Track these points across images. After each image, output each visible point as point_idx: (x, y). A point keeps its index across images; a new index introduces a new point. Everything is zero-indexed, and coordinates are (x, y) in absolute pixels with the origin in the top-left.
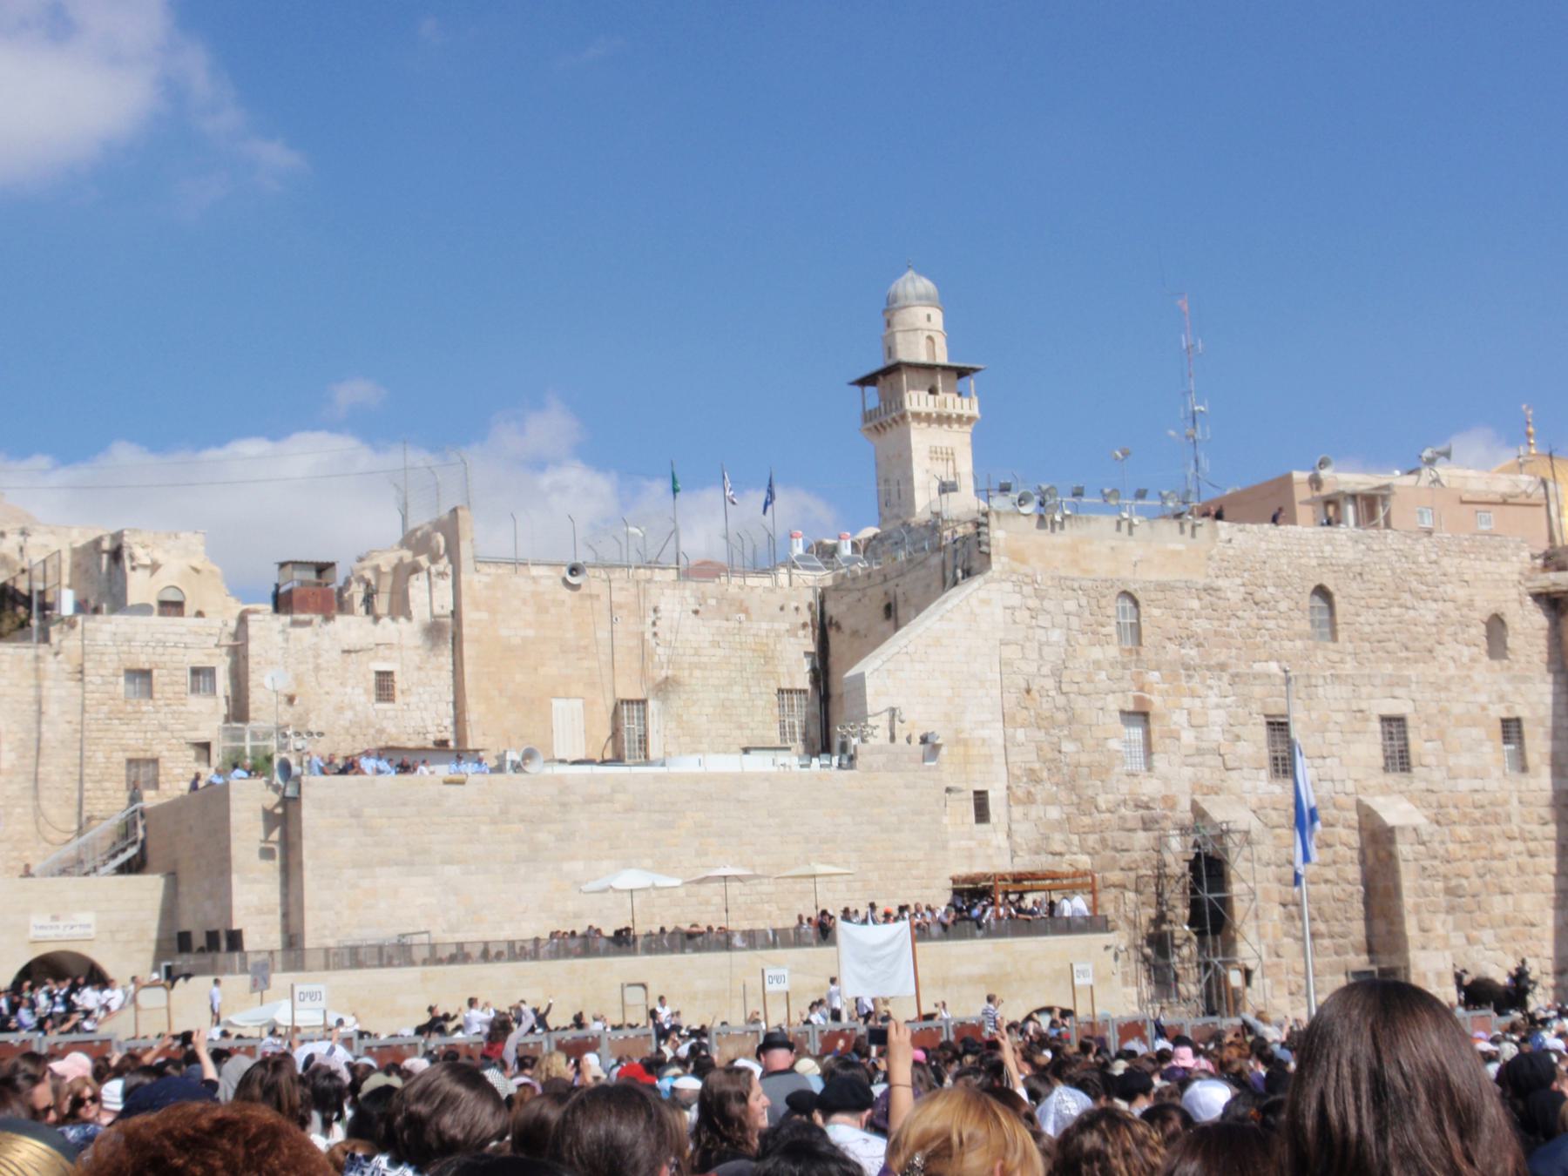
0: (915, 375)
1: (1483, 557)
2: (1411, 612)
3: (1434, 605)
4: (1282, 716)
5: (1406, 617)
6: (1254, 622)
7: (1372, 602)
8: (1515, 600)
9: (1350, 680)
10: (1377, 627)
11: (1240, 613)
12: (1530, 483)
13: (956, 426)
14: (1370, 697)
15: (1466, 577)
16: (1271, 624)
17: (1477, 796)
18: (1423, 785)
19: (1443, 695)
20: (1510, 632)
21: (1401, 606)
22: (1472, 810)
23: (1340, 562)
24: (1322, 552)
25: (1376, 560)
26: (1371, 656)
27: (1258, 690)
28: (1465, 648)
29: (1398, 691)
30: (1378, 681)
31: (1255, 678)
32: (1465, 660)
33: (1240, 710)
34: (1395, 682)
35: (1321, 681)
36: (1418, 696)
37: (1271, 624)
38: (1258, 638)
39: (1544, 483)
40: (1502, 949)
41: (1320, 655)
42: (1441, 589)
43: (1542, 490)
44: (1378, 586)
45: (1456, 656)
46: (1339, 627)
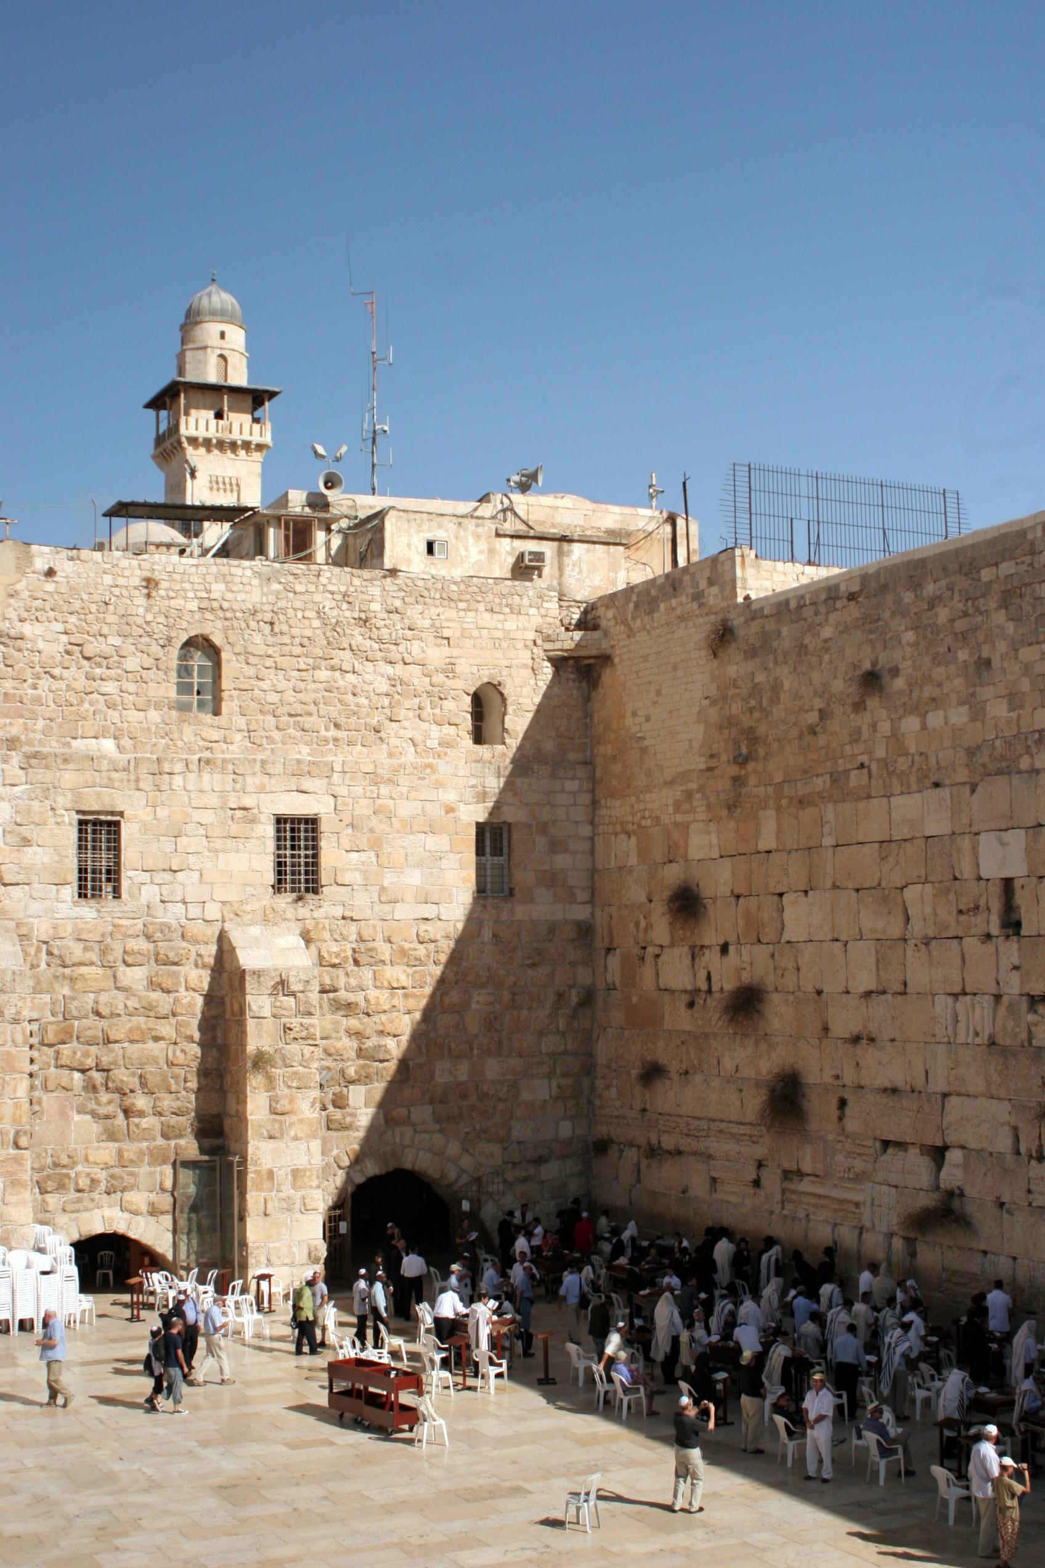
0: (198, 396)
1: (481, 607)
2: (350, 677)
3: (389, 670)
4: (112, 813)
5: (341, 683)
6: (81, 683)
7: (283, 662)
8: (525, 666)
9: (230, 767)
10: (290, 696)
11: (57, 671)
12: (652, 518)
13: (242, 453)
14: (262, 790)
15: (446, 633)
16: (110, 687)
17: (423, 927)
18: (339, 911)
19: (384, 790)
20: (510, 709)
21: (333, 669)
22: (416, 945)
23: (236, 606)
24: (209, 592)
25: (298, 604)
26: (276, 735)
27: (69, 778)
28: (434, 727)
29: (308, 784)
30: (277, 769)
31: (66, 760)
32: (433, 743)
33: (36, 804)
34: (301, 771)
35: (179, 767)
36: (343, 791)
37: (110, 687)
38: (86, 705)
39: (672, 520)
40: (441, 1131)
41: (188, 731)
42: (401, 648)
43: (668, 528)
44: (297, 641)
45: (419, 738)
46: (225, 695)
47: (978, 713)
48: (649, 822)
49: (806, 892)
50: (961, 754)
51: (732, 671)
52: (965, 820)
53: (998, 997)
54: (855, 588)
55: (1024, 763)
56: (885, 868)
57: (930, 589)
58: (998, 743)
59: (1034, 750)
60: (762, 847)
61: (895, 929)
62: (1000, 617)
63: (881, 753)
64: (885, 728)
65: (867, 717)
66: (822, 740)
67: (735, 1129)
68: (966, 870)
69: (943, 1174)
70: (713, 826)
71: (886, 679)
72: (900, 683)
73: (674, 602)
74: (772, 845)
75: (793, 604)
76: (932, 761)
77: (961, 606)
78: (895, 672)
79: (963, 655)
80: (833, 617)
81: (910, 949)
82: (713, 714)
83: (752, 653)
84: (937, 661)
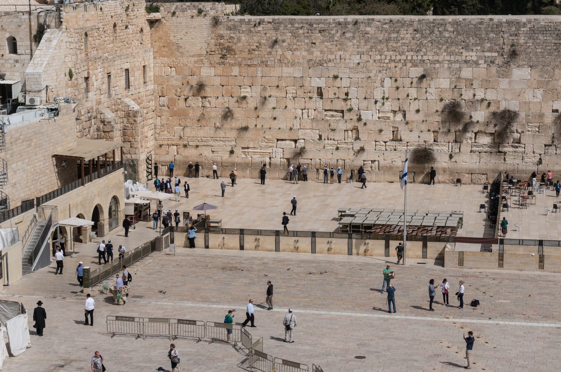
47: (312, 53)
48: (182, 65)
49: (250, 86)
50: (305, 61)
51: (222, 32)
52: (307, 74)
53: (315, 110)
54: (271, 21)
55: (325, 65)
56: (280, 82)
57: (297, 25)
58: (317, 60)
59: (328, 62)
60: (232, 74)
61: (284, 95)
62: (319, 35)
63: (279, 58)
64: (280, 52)
65: (274, 50)
66: (257, 53)
67: (222, 139)
68: (306, 84)
69: (297, 144)
70: (213, 69)
71: (280, 43)
72: (285, 44)
73: (194, 11)
74: (237, 74)
75: (247, 20)
76: (296, 61)
77: (306, 31)
78: (284, 41)
79: (306, 41)
80: (261, 26)
81: (288, 100)
82: (213, 41)
83: (229, 28)
84: (298, 41)
